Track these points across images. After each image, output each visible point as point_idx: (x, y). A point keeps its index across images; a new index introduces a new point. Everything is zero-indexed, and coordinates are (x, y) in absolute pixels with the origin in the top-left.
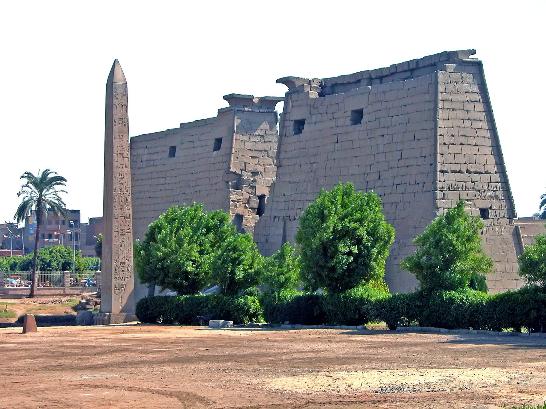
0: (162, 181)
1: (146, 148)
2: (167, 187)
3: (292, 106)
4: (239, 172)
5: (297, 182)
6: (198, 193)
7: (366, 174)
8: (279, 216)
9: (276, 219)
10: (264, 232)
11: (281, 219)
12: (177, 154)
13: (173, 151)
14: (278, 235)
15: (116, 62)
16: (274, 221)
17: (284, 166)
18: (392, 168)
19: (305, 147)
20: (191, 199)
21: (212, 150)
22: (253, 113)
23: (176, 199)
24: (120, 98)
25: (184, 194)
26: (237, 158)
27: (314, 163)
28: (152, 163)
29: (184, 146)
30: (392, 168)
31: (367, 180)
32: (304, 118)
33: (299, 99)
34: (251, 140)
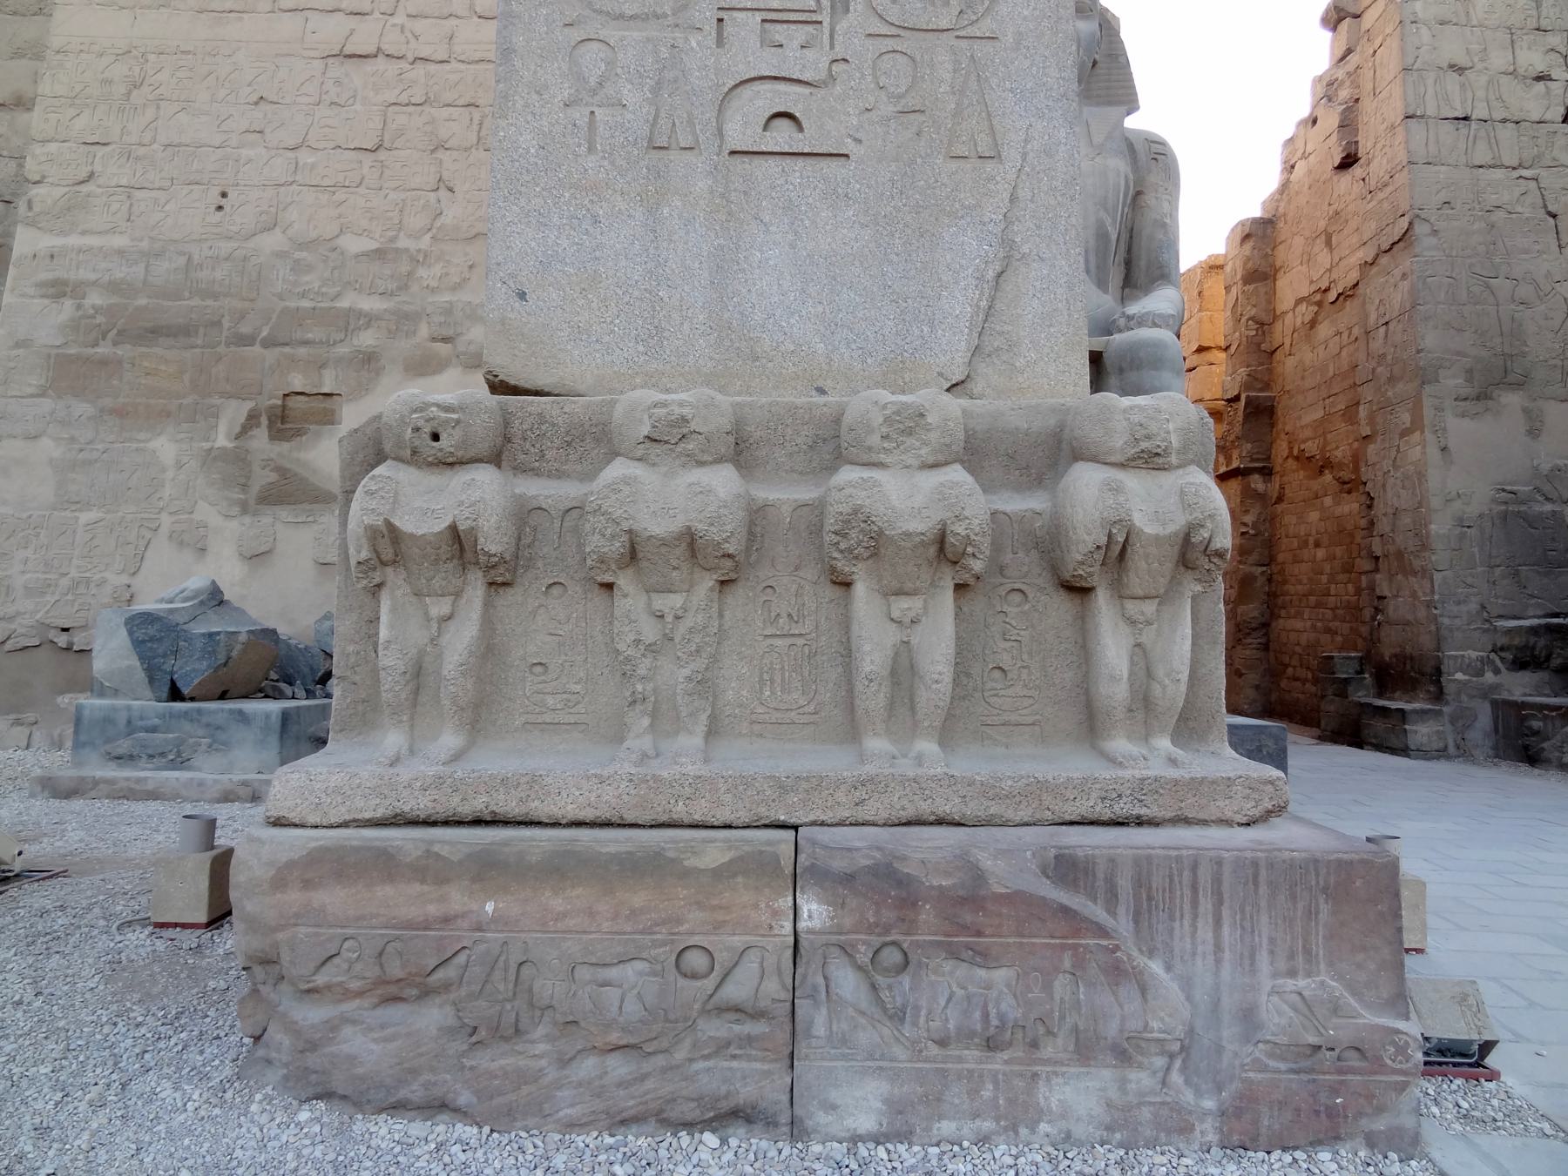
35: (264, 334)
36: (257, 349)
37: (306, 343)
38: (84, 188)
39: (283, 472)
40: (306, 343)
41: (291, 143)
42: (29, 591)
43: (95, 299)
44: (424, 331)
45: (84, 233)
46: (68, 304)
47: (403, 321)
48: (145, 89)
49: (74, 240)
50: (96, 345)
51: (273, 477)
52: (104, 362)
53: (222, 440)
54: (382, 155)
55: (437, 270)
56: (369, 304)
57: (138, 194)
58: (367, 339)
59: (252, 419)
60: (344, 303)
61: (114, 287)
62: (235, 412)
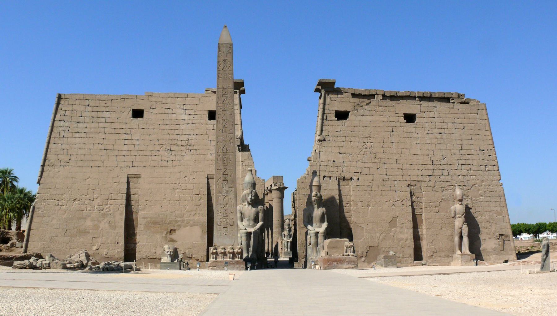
1: (88, 105)
3: (331, 101)
7: (430, 156)
16: (324, 179)
17: (329, 141)
18: (454, 154)
19: (353, 130)
21: (208, 119)
27: (368, 142)
30: (454, 154)
31: (432, 159)
32: (348, 110)
35: (168, 223)
36: (167, 225)
37: (172, 224)
38: (146, 206)
39: (171, 239)
40: (172, 224)
41: (169, 200)
42: (144, 252)
43: (149, 219)
44: (185, 222)
45: (146, 211)
46: (146, 219)
47: (183, 221)
48: (152, 194)
49: (145, 212)
50: (149, 224)
51: (170, 239)
52: (150, 226)
53: (164, 235)
54: (179, 201)
55: (187, 215)
56: (179, 219)
57: (152, 206)
58: (179, 223)
59: (167, 233)
60: (176, 219)
61: (150, 218)
62: (165, 232)
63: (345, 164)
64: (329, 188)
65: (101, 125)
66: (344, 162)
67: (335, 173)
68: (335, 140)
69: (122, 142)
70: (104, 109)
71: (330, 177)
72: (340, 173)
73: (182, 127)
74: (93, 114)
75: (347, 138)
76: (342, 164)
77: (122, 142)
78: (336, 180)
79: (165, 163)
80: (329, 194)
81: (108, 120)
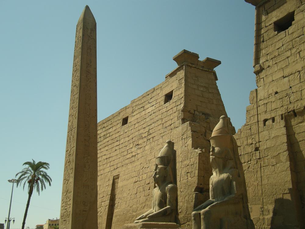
0: (118, 143)
2: (121, 146)
4: (192, 111)
5: (299, 71)
6: (151, 139)
8: (273, 116)
9: (269, 123)
10: (250, 141)
11: (278, 119)
12: (129, 121)
13: (125, 121)
14: (277, 137)
15: (87, 8)
16: (265, 125)
20: (145, 146)
22: (198, 70)
23: (130, 152)
24: (89, 31)
25: (137, 145)
26: (190, 100)
28: (108, 135)
29: (135, 114)
32: (291, 11)
33: (277, 2)
34: (199, 89)
63: (294, 89)
64: (273, 135)
65: (107, 140)
66: (291, 87)
67: (279, 109)
68: (276, 62)
69: (114, 149)
70: (110, 127)
71: (273, 119)
72: (286, 107)
73: (148, 120)
74: (105, 133)
75: (294, 51)
76: (290, 91)
77: (114, 149)
78: (282, 119)
79: (133, 158)
80: (273, 145)
81: (111, 134)
